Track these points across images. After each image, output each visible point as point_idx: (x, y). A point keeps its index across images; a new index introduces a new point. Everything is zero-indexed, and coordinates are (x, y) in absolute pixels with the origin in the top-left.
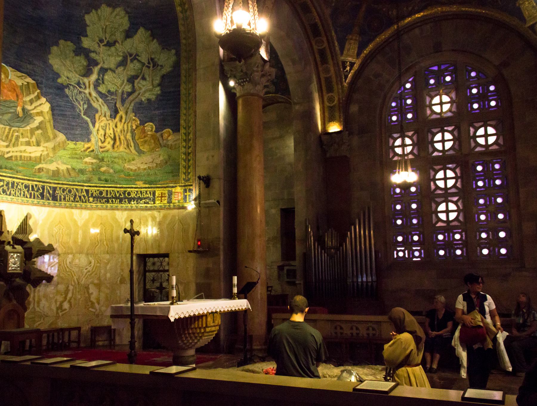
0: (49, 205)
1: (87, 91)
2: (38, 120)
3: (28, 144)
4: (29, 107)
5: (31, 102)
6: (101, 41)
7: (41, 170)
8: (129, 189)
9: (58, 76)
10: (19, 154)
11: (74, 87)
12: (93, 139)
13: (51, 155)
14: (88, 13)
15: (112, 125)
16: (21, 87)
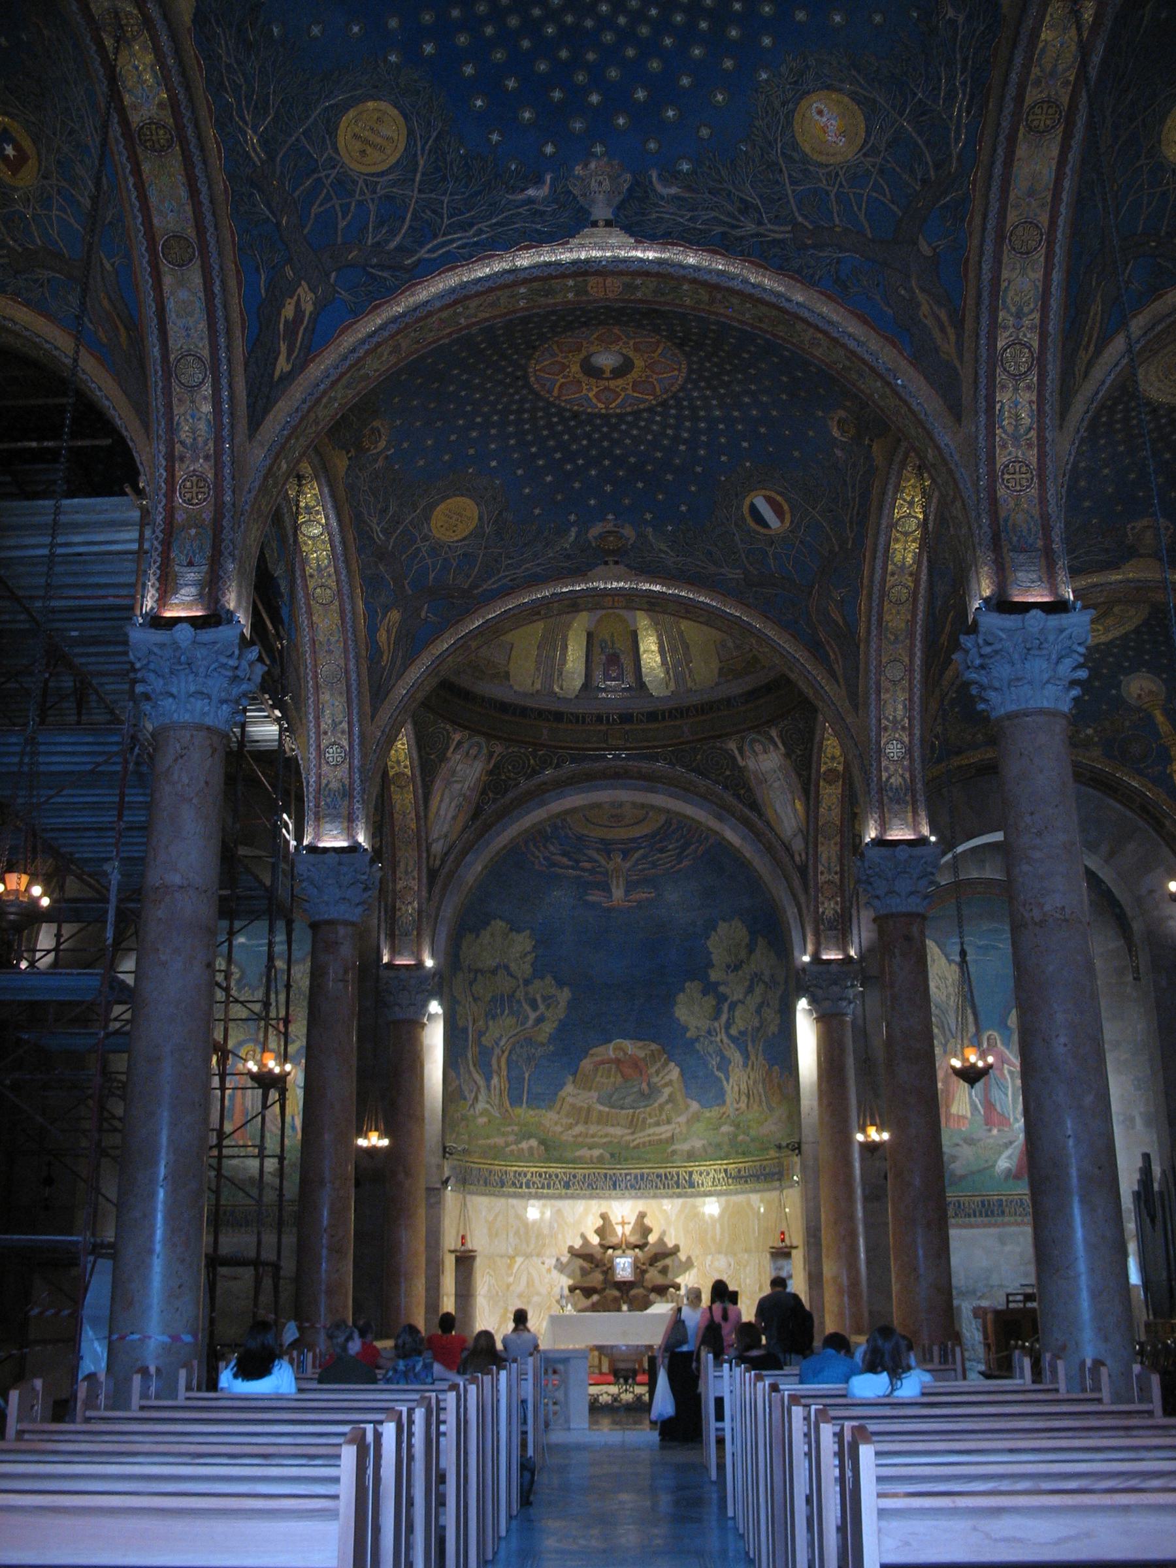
0: (685, 1195)
1: (718, 1039)
2: (667, 1091)
3: (657, 1124)
4: (655, 1080)
5: (657, 1073)
6: (728, 967)
7: (674, 1152)
8: (765, 1163)
9: (685, 1029)
10: (647, 1139)
11: (705, 1037)
12: (728, 1101)
13: (684, 1131)
14: (708, 938)
15: (746, 1078)
16: (644, 1059)
